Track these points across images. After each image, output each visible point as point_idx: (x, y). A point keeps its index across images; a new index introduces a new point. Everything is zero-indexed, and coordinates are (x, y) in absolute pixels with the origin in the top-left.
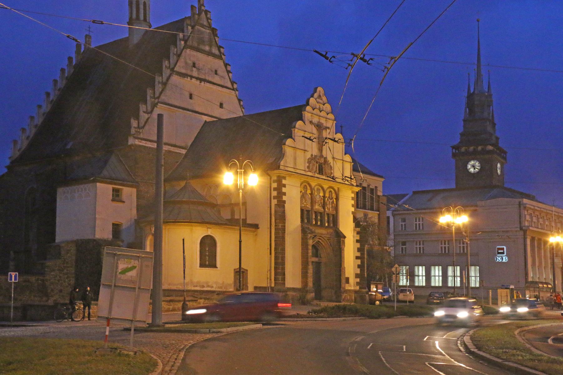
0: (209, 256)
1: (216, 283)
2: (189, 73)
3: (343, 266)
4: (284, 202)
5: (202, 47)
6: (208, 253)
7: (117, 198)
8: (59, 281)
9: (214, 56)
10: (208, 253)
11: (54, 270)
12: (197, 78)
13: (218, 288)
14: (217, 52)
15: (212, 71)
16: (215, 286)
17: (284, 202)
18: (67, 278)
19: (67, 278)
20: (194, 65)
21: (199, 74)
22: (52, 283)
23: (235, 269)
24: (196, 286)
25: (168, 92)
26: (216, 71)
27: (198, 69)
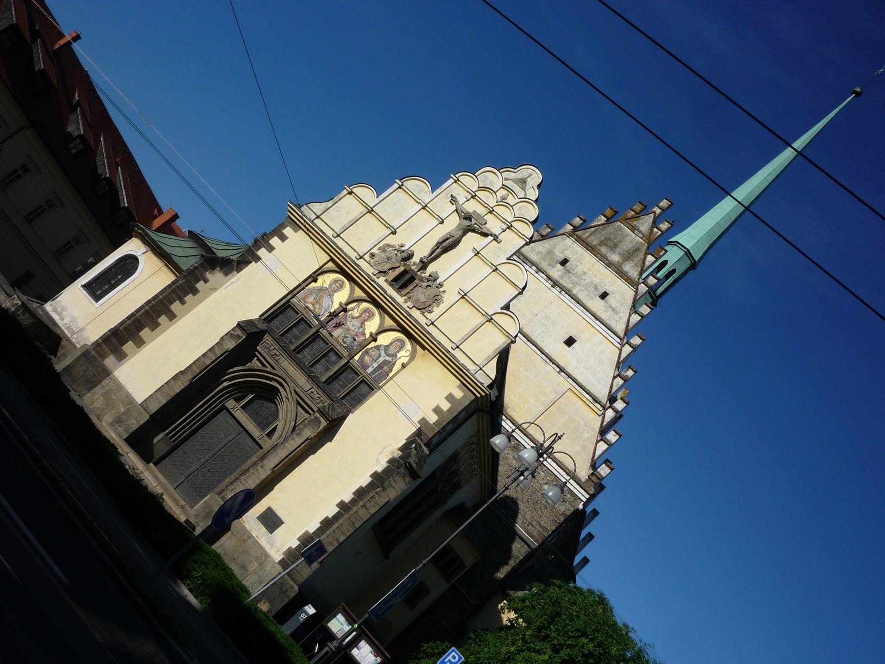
1: (73, 319)
2: (544, 265)
4: (258, 259)
5: (603, 250)
12: (549, 278)
13: (69, 328)
14: (633, 273)
15: (596, 288)
16: (67, 320)
21: (562, 278)
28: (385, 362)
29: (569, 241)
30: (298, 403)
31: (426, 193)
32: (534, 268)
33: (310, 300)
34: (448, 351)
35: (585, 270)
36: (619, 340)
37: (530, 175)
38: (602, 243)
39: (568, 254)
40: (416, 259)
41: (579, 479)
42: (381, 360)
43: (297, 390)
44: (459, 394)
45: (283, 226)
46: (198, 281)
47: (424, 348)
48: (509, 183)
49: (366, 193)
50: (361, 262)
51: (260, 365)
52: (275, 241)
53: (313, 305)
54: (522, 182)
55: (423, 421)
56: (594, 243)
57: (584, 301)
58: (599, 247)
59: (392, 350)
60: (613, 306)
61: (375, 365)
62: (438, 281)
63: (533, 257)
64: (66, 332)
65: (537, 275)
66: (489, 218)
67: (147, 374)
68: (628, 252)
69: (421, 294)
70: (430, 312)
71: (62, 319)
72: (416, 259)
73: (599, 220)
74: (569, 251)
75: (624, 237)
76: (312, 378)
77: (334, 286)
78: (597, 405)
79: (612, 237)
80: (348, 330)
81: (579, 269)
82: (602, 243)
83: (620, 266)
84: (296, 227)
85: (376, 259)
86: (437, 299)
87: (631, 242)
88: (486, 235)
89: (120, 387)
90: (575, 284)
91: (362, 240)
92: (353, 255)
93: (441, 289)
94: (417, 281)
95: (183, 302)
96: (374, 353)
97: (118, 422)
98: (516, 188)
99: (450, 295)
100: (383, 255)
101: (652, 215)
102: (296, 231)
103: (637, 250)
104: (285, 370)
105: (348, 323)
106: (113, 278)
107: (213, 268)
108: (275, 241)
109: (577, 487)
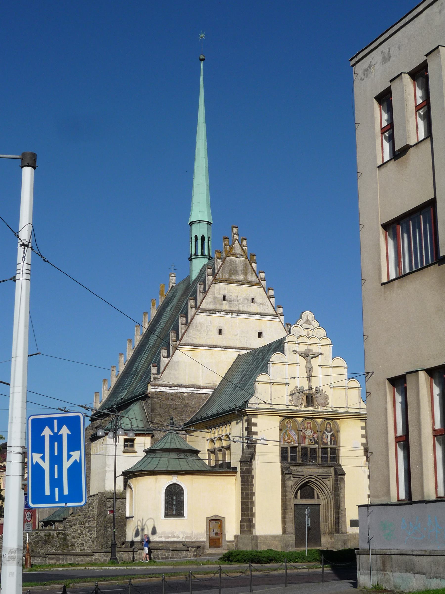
0: (176, 504)
2: (218, 307)
3: (341, 508)
5: (234, 277)
6: (174, 502)
7: (129, 449)
8: (80, 534)
9: (251, 284)
10: (174, 502)
11: (75, 524)
12: (227, 312)
13: (186, 538)
14: (254, 279)
15: (248, 300)
18: (88, 532)
19: (88, 532)
20: (224, 298)
21: (231, 307)
22: (73, 537)
23: (207, 518)
24: (161, 537)
25: (191, 331)
26: (253, 299)
27: (230, 301)
28: (331, 436)
29: (217, 285)
30: (322, 478)
31: (282, 357)
32: (217, 312)
33: (286, 439)
34: (346, 412)
35: (236, 294)
36: (277, 317)
37: (308, 316)
38: (231, 274)
39: (223, 292)
40: (306, 388)
42: (329, 436)
43: (318, 474)
44: (363, 424)
47: (339, 419)
48: (305, 326)
49: (261, 377)
50: (290, 408)
51: (297, 479)
52: (254, 429)
53: (289, 439)
54: (308, 322)
55: (363, 444)
56: (227, 277)
57: (249, 310)
58: (231, 278)
59: (329, 429)
60: (261, 302)
61: (329, 440)
62: (321, 390)
63: (211, 307)
64: (187, 540)
65: (221, 315)
66: (311, 348)
67: (270, 522)
68: (243, 270)
69: (319, 400)
71: (179, 537)
72: (306, 388)
73: (219, 263)
74: (221, 290)
75: (236, 263)
76: (320, 465)
77: (288, 425)
79: (231, 267)
80: (309, 436)
81: (233, 297)
82: (231, 274)
83: (247, 280)
84: (255, 416)
85: (294, 401)
86: (326, 398)
87: (241, 263)
88: (318, 356)
89: (266, 537)
90: (238, 305)
91: (281, 398)
93: (324, 392)
97: (287, 547)
98: (308, 326)
99: (329, 392)
100: (294, 397)
101: (236, 241)
102: (257, 418)
103: (246, 265)
104: (308, 472)
106: (172, 502)
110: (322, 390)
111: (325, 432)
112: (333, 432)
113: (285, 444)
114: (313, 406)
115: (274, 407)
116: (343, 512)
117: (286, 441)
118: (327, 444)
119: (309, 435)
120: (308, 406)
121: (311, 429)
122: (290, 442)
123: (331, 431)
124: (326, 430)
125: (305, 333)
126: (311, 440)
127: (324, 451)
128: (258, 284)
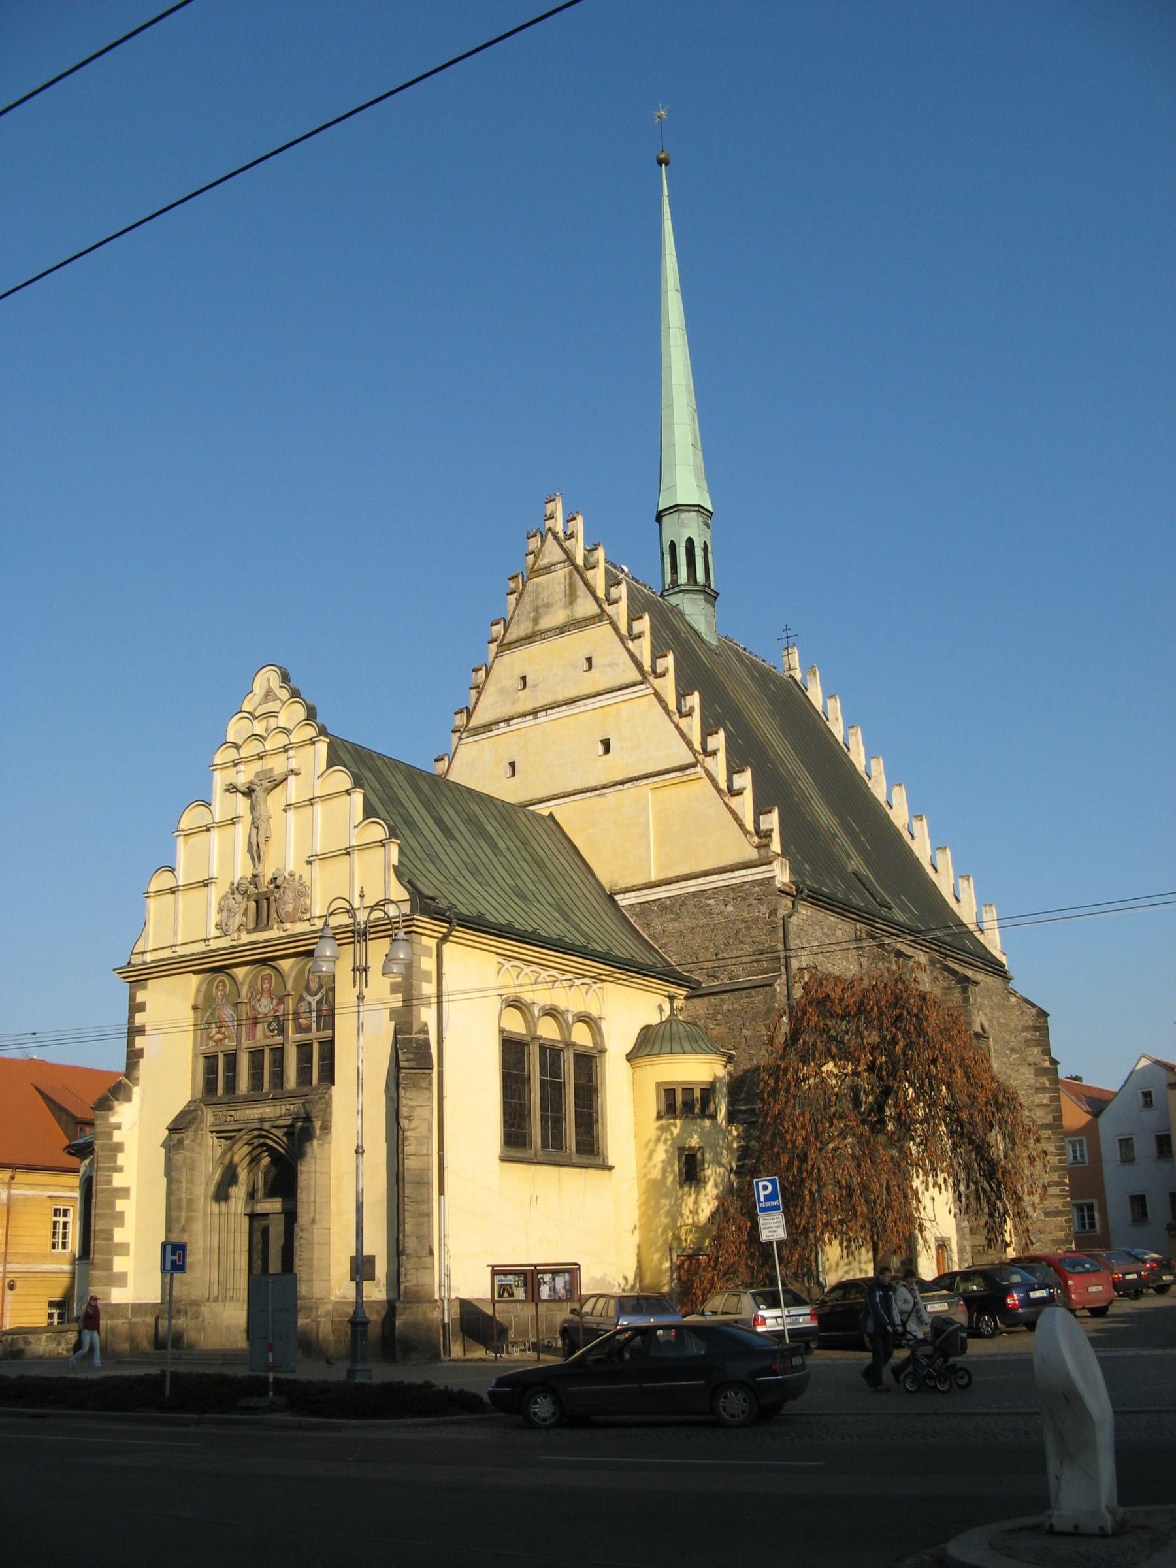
5: (545, 623)
15: (576, 667)
17: (140, 1053)
28: (319, 1002)
29: (507, 658)
32: (502, 725)
39: (519, 673)
41: (751, 861)
42: (314, 1006)
45: (132, 997)
46: (110, 1135)
52: (139, 1019)
55: (394, 1014)
56: (529, 631)
58: (537, 628)
59: (314, 986)
70: (306, 911)
78: (688, 772)
92: (200, 947)
93: (297, 877)
94: (272, 898)
95: (120, 1169)
96: (303, 1007)
102: (145, 988)
105: (260, 1010)
107: (110, 1108)
108: (139, 1019)
109: (754, 870)
110: (292, 875)
111: (305, 994)
112: (324, 991)
113: (211, 1047)
114: (268, 927)
115: (181, 951)
116: (304, 1235)
117: (211, 1038)
118: (308, 1029)
119: (266, 1010)
120: (256, 929)
121: (270, 995)
122: (221, 1040)
123: (320, 987)
124: (308, 989)
125: (259, 728)
126: (270, 1024)
127: (304, 1049)
128: (601, 616)
